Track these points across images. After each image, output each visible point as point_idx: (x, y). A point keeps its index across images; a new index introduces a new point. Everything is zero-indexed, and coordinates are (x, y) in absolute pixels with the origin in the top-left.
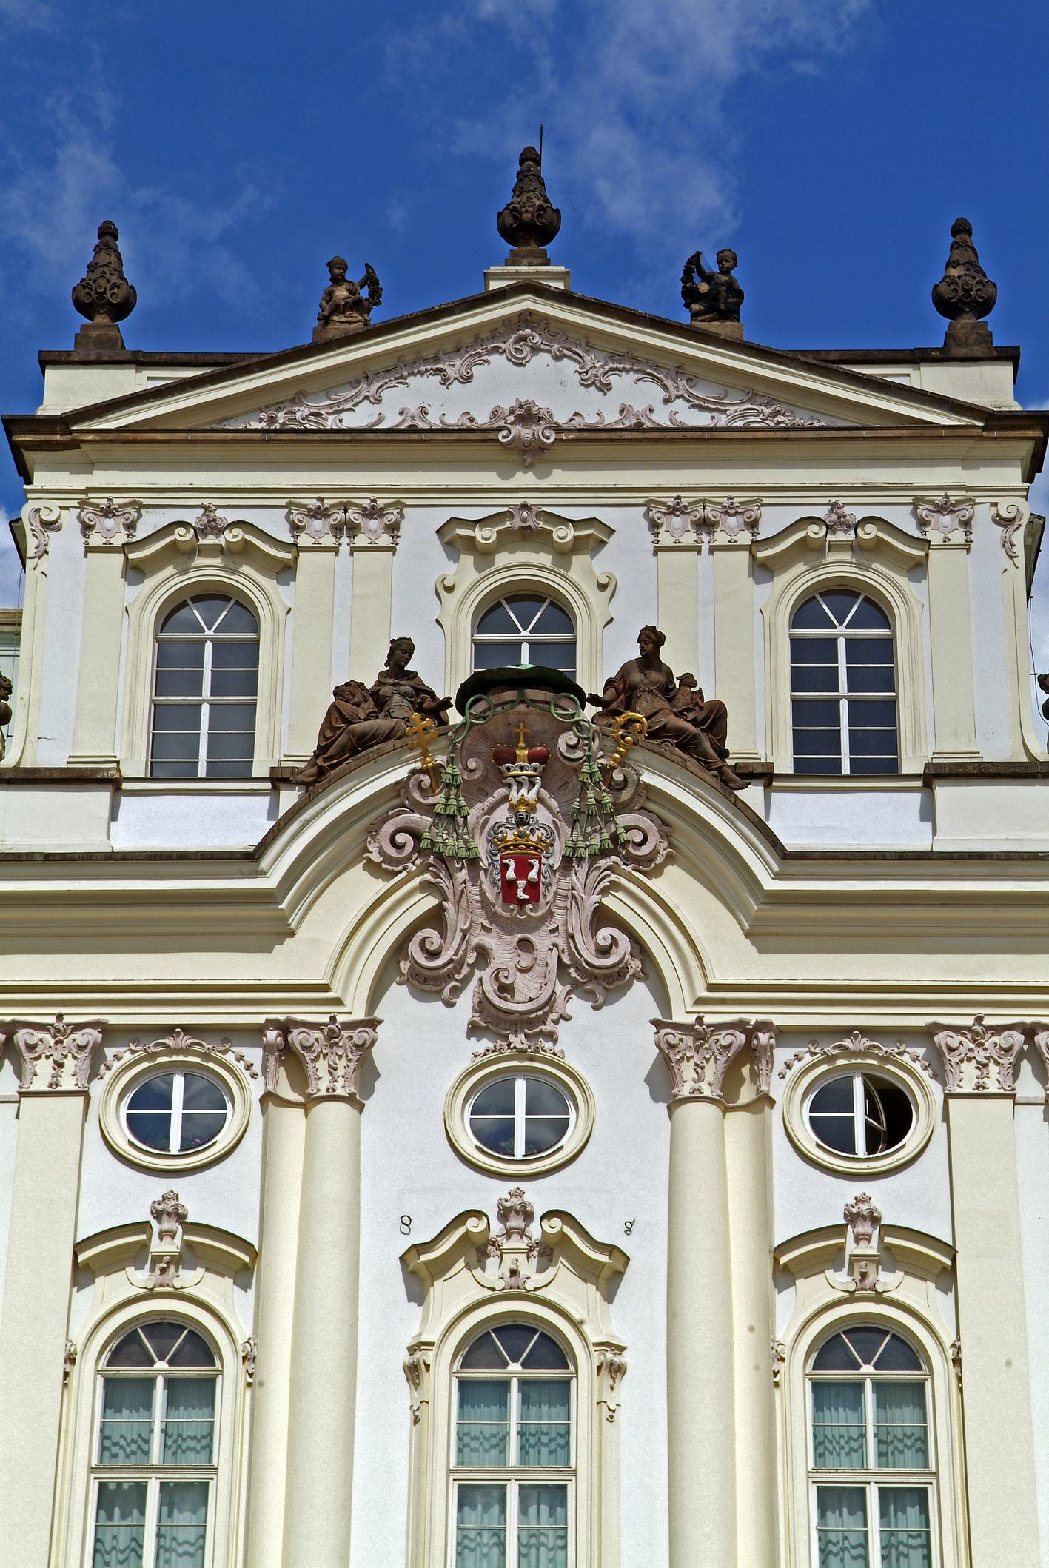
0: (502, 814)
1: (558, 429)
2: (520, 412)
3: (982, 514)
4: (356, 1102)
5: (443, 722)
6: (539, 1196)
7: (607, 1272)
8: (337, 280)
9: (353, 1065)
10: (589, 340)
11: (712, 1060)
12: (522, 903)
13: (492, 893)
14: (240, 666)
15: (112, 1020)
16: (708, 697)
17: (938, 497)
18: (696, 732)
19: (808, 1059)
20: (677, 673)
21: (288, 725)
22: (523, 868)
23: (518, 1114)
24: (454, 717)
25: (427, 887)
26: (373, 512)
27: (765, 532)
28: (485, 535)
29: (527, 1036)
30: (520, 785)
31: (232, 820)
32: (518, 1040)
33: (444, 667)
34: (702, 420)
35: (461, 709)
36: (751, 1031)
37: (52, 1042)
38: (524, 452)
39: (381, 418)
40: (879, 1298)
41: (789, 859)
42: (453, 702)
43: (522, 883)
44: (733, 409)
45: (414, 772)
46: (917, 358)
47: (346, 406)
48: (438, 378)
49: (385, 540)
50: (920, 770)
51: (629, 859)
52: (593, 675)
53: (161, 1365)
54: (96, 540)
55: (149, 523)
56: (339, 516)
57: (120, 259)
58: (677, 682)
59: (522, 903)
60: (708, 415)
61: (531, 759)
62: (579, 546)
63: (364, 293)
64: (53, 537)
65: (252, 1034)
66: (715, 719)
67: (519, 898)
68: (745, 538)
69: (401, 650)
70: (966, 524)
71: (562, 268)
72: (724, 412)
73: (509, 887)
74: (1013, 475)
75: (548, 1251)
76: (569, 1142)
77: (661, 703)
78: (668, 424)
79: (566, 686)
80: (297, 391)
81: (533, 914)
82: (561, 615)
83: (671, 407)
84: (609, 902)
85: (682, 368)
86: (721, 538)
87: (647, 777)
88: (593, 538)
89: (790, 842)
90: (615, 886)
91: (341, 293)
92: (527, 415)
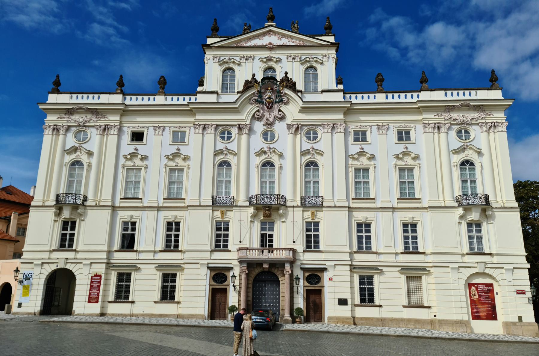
6: (271, 146)
7: (281, 156)
8: (246, 26)
10: (279, 33)
14: (233, 78)
18: (292, 86)
21: (239, 86)
22: (269, 104)
24: (261, 84)
31: (233, 98)
32: (269, 127)
33: (259, 78)
34: (294, 44)
40: (314, 158)
46: (322, 35)
49: (252, 61)
52: (279, 78)
54: (214, 61)
66: (294, 84)
68: (299, 60)
73: (267, 107)
74: (334, 51)
76: (275, 139)
80: (240, 41)
85: (291, 37)
86: (296, 60)
87: (286, 92)
88: (279, 61)
92: (270, 44)
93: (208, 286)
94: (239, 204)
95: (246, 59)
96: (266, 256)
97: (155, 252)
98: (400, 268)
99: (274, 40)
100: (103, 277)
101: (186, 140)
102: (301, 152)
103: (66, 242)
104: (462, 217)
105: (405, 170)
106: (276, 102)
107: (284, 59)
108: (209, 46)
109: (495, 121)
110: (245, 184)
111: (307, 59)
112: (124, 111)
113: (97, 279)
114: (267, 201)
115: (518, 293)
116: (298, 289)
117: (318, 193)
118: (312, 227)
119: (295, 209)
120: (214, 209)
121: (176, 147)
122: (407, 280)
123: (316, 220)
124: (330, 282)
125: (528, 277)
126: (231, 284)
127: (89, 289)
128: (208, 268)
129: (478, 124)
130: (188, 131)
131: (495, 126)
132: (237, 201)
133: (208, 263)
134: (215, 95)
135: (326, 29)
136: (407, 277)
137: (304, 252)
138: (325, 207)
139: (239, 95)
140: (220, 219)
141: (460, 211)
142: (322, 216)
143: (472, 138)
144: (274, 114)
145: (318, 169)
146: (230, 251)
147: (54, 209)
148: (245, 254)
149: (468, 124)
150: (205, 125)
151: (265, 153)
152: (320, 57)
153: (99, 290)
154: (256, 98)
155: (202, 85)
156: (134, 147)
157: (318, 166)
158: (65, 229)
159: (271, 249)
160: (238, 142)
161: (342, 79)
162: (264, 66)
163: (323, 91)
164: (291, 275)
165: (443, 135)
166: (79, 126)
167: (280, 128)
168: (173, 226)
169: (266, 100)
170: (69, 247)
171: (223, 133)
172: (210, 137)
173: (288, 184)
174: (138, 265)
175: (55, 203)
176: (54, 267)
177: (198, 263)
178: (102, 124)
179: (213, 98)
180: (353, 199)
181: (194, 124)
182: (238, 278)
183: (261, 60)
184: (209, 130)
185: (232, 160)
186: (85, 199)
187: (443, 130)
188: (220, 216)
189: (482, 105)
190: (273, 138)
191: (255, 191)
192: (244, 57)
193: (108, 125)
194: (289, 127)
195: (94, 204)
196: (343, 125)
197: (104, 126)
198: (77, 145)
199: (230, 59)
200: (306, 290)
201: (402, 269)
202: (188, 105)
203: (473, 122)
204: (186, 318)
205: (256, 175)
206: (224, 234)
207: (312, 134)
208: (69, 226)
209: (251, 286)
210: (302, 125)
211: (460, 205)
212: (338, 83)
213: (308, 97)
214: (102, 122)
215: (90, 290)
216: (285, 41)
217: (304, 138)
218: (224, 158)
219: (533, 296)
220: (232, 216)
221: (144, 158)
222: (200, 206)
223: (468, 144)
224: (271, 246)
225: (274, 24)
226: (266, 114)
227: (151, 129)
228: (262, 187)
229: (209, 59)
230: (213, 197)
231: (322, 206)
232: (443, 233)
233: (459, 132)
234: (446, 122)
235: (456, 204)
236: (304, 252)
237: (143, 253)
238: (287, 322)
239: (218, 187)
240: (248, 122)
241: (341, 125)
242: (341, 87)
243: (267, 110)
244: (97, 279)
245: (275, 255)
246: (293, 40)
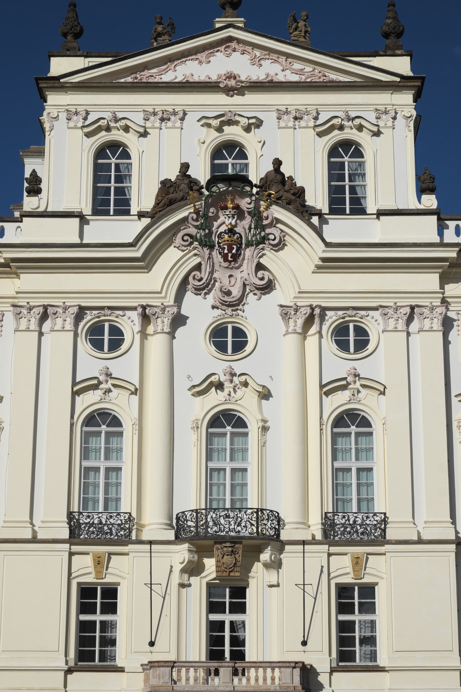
1: (242, 82)
2: (227, 75)
4: (172, 335)
5: (201, 194)
8: (160, 23)
9: (170, 321)
11: (300, 318)
12: (230, 262)
15: (83, 304)
16: (298, 185)
17: (382, 108)
18: (294, 198)
19: (334, 318)
20: (287, 175)
21: (143, 195)
23: (229, 339)
25: (195, 255)
26: (175, 113)
29: (232, 310)
30: (229, 217)
33: (201, 173)
34: (295, 78)
35: (207, 190)
37: (61, 312)
38: (229, 91)
39: (176, 78)
41: (328, 245)
42: (204, 187)
43: (230, 255)
44: (307, 74)
45: (190, 213)
46: (375, 54)
47: (163, 73)
48: (197, 62)
49: (178, 124)
50: (375, 212)
51: (270, 244)
53: (104, 427)
56: (160, 115)
57: (77, 15)
58: (287, 179)
59: (230, 262)
60: (298, 76)
61: (233, 208)
63: (169, 29)
64: (55, 123)
66: (301, 192)
68: (312, 124)
69: (185, 167)
70: (394, 118)
71: (242, 19)
72: (304, 75)
77: (280, 186)
78: (283, 80)
79: (245, 180)
81: (234, 266)
83: (284, 73)
84: (262, 261)
86: (303, 123)
89: (328, 240)
90: (264, 255)
91: (160, 28)
92: (231, 76)
94: (145, 536)
95: (162, 120)
99: (240, 65)
102: (322, 386)
106: (249, 244)
107: (269, 118)
108: (58, 84)
110: (160, 478)
111: (335, 121)
114: (228, 527)
117: (370, 500)
118: (356, 601)
119: (307, 547)
120: (75, 548)
123: (367, 580)
132: (140, 528)
135: (386, 35)
137: (332, 671)
142: (384, 569)
144: (245, 275)
145: (371, 434)
146: (121, 670)
148: (167, 678)
150: (45, 307)
151: (220, 386)
152: (371, 116)
154: (193, 231)
155: (35, 190)
159: (239, 665)
160: (144, 358)
161: (433, 179)
162: (213, 138)
163: (380, 214)
167: (258, 316)
169: (220, 236)
172: (59, 340)
173: (286, 480)
179: (67, 231)
181: (14, 306)
184: (59, 321)
185: (122, 405)
188: (91, 569)
190: (239, 346)
191: (190, 498)
192: (155, 114)
194: (286, 312)
196: (439, 310)
199: (116, 120)
205: (194, 452)
207: (351, 338)
210: (324, 310)
212: (423, 189)
213: (341, 229)
216: (271, 70)
217: (330, 346)
218: (100, 401)
220: (127, 570)
222: (34, 540)
224: (239, 656)
225: (240, 21)
228: (209, 487)
230: (70, 515)
236: (332, 671)
239: (85, 487)
240: (170, 300)
241: (432, 309)
242: (430, 201)
243: (226, 264)
245: (253, 681)
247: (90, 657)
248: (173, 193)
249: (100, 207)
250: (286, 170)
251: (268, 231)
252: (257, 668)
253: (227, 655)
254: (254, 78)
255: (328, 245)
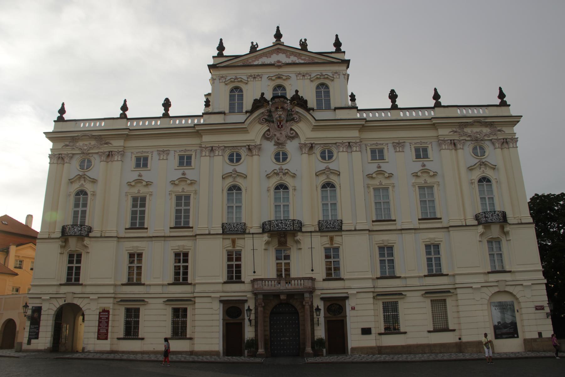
0: (277, 116)
3: (341, 74)
5: (269, 104)
6: (284, 167)
13: (276, 127)
14: (241, 97)
21: (248, 105)
23: (281, 157)
27: (312, 76)
28: (274, 78)
31: (240, 118)
32: (280, 146)
33: (268, 96)
34: (302, 62)
36: (312, 144)
41: (316, 120)
51: (295, 121)
52: (289, 96)
55: (228, 78)
62: (287, 79)
65: (245, 146)
66: (306, 102)
67: (280, 127)
68: (309, 77)
69: (263, 94)
73: (278, 126)
75: (285, 174)
76: (288, 160)
82: (284, 89)
84: (292, 127)
86: (306, 78)
88: (288, 78)
92: (279, 62)
93: (221, 321)
94: (252, 231)
96: (283, 287)
97: (163, 285)
98: (424, 292)
100: (111, 313)
101: (193, 164)
103: (73, 276)
104: (482, 235)
105: (424, 188)
106: (287, 121)
109: (506, 137)
110: (258, 209)
112: (127, 135)
113: (106, 315)
115: (537, 309)
116: (318, 320)
119: (313, 234)
121: (182, 171)
122: (432, 304)
124: (353, 311)
125: (545, 292)
126: (246, 318)
127: (97, 325)
128: (221, 301)
129: (491, 140)
130: (194, 154)
131: (507, 143)
133: (221, 296)
134: (222, 116)
136: (431, 301)
138: (344, 231)
139: (248, 114)
140: (230, 248)
141: (481, 229)
143: (486, 154)
146: (243, 282)
147: (59, 243)
149: (482, 140)
150: (212, 147)
151: (277, 174)
153: (108, 326)
154: (266, 117)
156: (137, 173)
157: (335, 187)
158: (70, 262)
162: (273, 84)
164: (311, 306)
165: (460, 151)
166: (83, 153)
167: (291, 147)
168: (182, 257)
169: (276, 119)
170: (75, 281)
171: (231, 155)
174: (146, 300)
175: (60, 235)
176: (62, 302)
177: (210, 297)
178: (105, 150)
179: (218, 119)
180: (373, 221)
182: (253, 312)
183: (270, 78)
184: (217, 152)
186: (90, 230)
187: (459, 146)
189: (493, 122)
190: (285, 159)
193: (112, 152)
195: (99, 235)
197: (108, 153)
198: (81, 173)
200: (328, 321)
201: (426, 293)
202: (194, 127)
203: (486, 138)
204: (200, 355)
206: (236, 265)
207: (327, 155)
208: (75, 259)
209: (268, 320)
211: (479, 224)
214: (106, 149)
215: (99, 326)
219: (551, 310)
221: (148, 184)
222: (209, 234)
223: (484, 160)
226: (278, 135)
227: (155, 154)
229: (215, 79)
231: (341, 230)
232: (465, 253)
233: (475, 149)
234: (462, 138)
235: (476, 223)
236: (324, 280)
237: (152, 287)
238: (309, 355)
244: (106, 315)
246: (303, 58)
247: (231, 278)
248: (259, 103)
249: (232, 111)
250: (300, 94)
251: (294, 116)
252: (295, 280)
253: (283, 276)
254: (287, 62)
255: (316, 120)
